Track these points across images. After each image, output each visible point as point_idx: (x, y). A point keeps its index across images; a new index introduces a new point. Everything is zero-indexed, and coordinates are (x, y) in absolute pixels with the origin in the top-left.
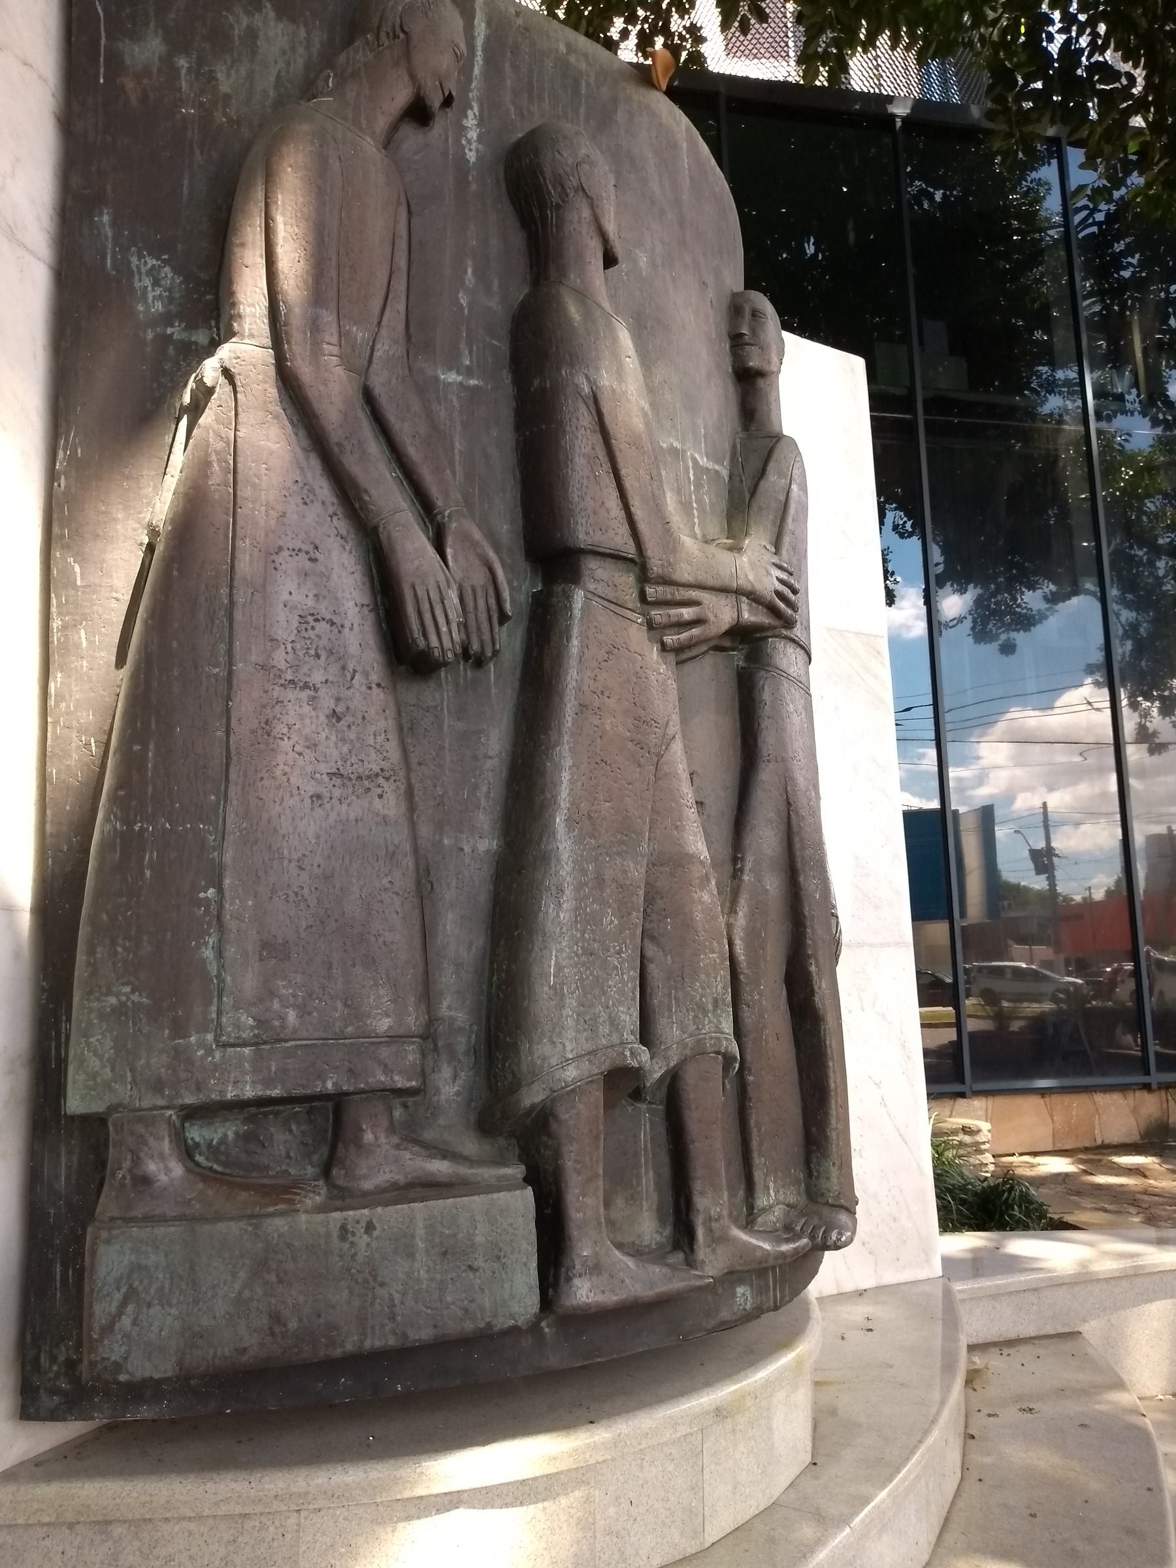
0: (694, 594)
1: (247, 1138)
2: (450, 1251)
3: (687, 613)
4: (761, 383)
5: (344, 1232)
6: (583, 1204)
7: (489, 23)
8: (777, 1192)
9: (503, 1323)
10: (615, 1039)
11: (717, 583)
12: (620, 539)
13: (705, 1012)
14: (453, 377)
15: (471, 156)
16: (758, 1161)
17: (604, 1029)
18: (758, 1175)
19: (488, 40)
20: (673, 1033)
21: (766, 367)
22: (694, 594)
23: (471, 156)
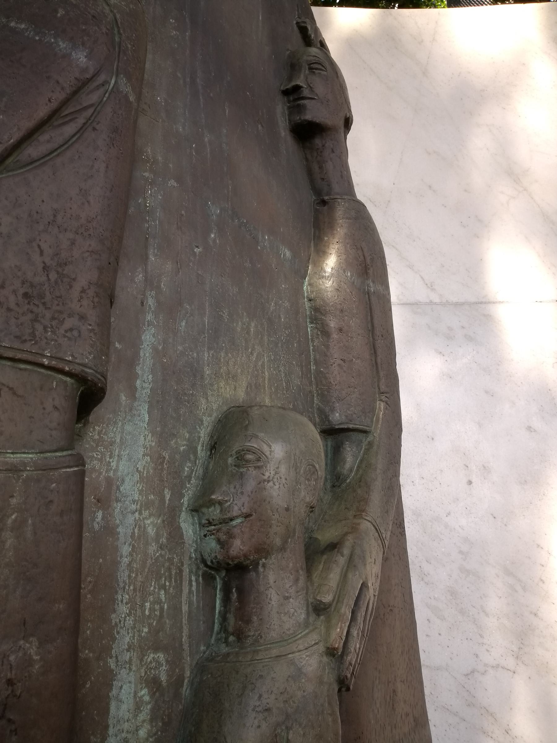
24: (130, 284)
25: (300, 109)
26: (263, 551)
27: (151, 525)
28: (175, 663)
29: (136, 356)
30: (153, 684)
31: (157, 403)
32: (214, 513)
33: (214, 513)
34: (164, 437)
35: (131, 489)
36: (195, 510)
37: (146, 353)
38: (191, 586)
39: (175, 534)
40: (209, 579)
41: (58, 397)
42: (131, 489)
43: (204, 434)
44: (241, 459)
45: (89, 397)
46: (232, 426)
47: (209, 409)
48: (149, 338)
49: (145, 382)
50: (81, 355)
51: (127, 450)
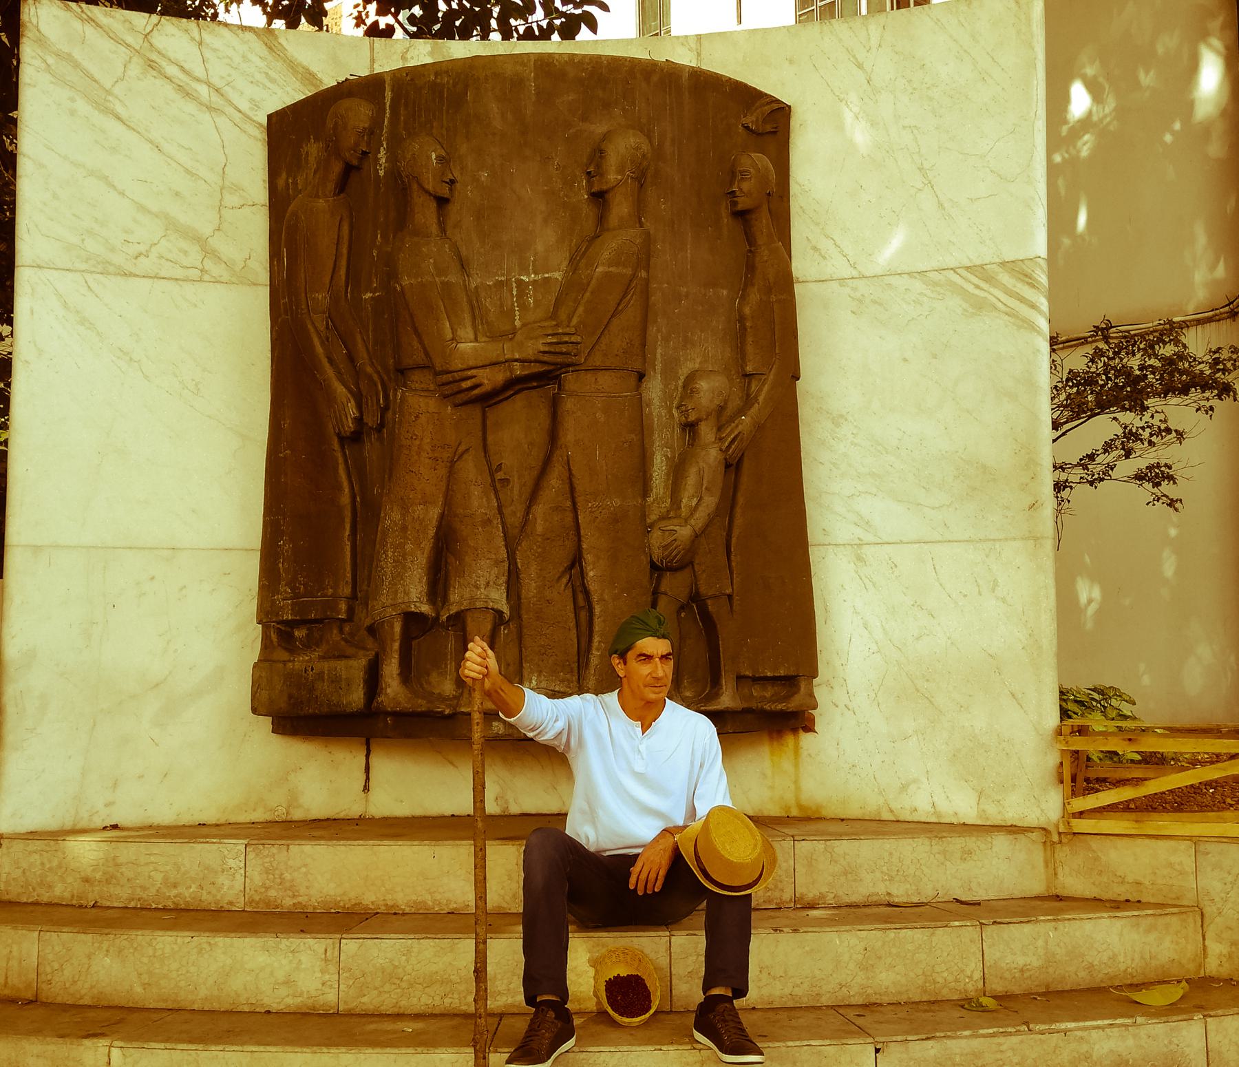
0: (469, 373)
1: (307, 635)
2: (335, 680)
3: (465, 385)
4: (606, 196)
5: (306, 670)
6: (391, 669)
7: (392, 91)
8: (539, 682)
9: (348, 710)
10: (406, 599)
11: (487, 362)
12: (419, 358)
13: (478, 588)
14: (369, 295)
15: (382, 173)
16: (526, 665)
17: (400, 595)
18: (525, 673)
19: (392, 99)
20: (458, 598)
21: (605, 188)
22: (469, 373)
23: (382, 173)
24: (652, 330)
25: (734, 204)
26: (699, 420)
27: (664, 412)
28: (673, 452)
29: (655, 359)
30: (667, 457)
31: (664, 372)
32: (683, 408)
33: (683, 408)
34: (666, 386)
35: (656, 401)
36: (677, 408)
37: (658, 356)
38: (677, 431)
39: (672, 416)
40: (684, 430)
41: (634, 376)
42: (656, 401)
43: (681, 383)
44: (692, 392)
45: (641, 376)
46: (691, 378)
47: (683, 373)
48: (659, 351)
49: (659, 367)
50: (638, 366)
51: (654, 389)
